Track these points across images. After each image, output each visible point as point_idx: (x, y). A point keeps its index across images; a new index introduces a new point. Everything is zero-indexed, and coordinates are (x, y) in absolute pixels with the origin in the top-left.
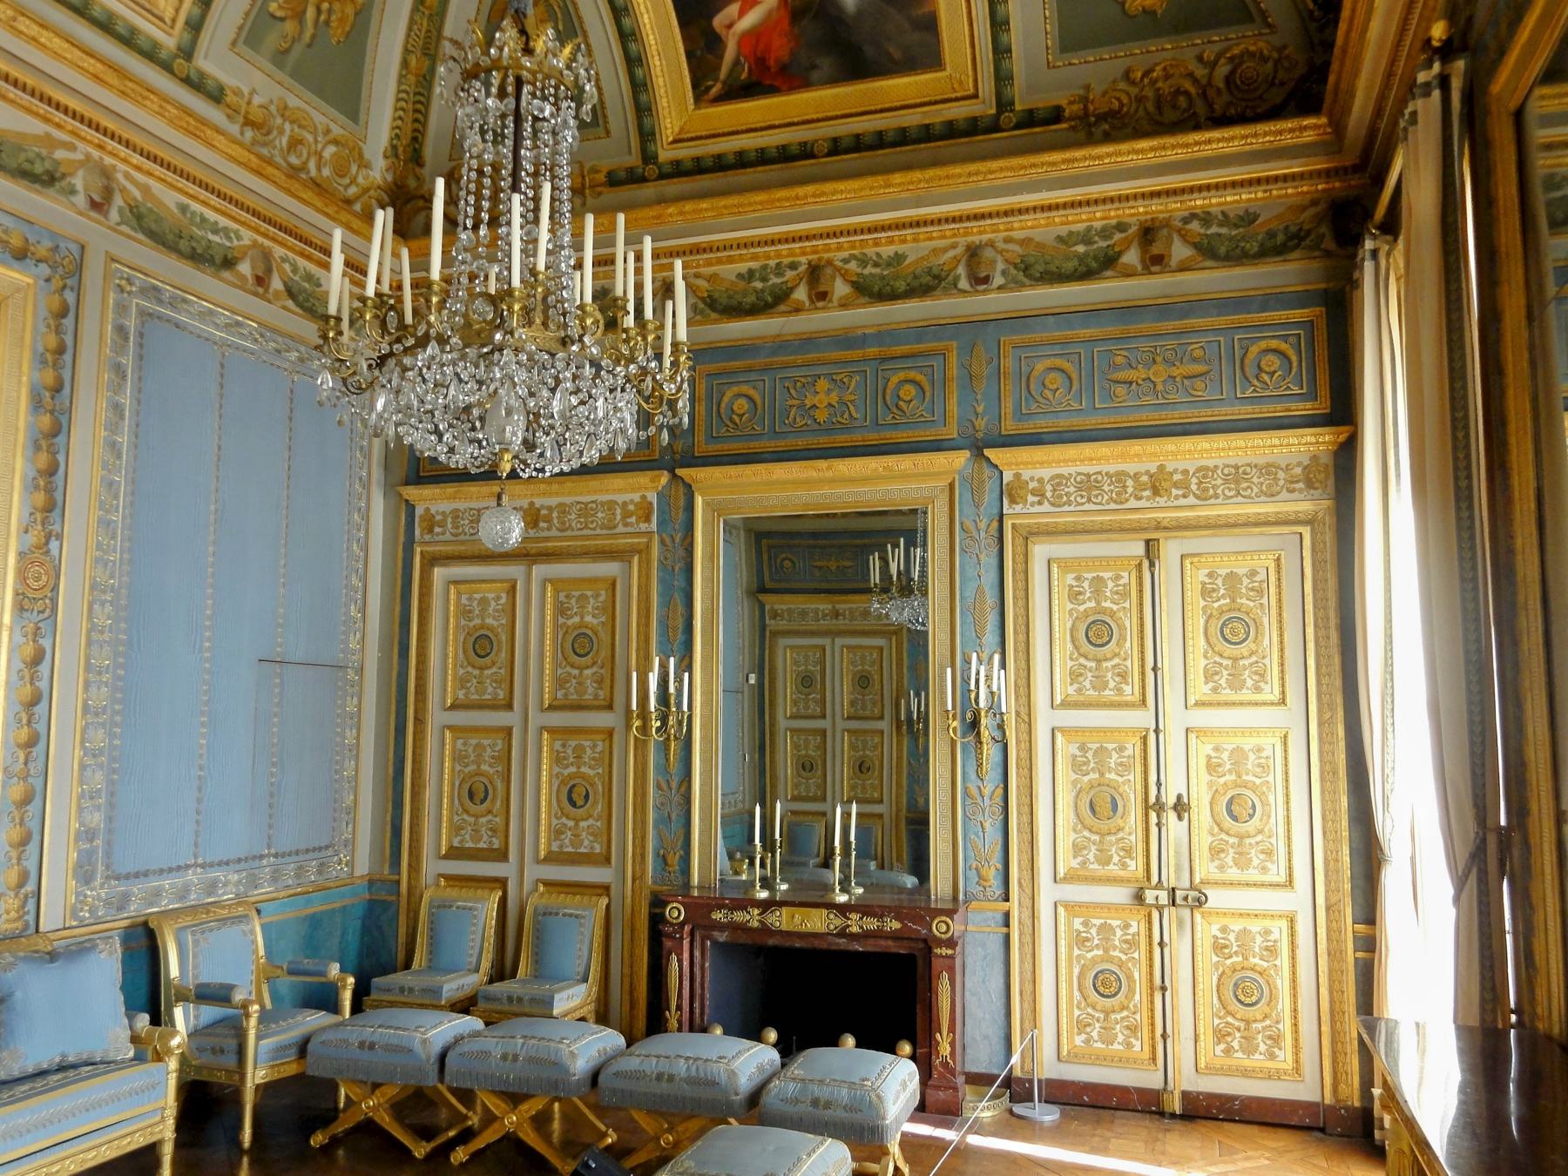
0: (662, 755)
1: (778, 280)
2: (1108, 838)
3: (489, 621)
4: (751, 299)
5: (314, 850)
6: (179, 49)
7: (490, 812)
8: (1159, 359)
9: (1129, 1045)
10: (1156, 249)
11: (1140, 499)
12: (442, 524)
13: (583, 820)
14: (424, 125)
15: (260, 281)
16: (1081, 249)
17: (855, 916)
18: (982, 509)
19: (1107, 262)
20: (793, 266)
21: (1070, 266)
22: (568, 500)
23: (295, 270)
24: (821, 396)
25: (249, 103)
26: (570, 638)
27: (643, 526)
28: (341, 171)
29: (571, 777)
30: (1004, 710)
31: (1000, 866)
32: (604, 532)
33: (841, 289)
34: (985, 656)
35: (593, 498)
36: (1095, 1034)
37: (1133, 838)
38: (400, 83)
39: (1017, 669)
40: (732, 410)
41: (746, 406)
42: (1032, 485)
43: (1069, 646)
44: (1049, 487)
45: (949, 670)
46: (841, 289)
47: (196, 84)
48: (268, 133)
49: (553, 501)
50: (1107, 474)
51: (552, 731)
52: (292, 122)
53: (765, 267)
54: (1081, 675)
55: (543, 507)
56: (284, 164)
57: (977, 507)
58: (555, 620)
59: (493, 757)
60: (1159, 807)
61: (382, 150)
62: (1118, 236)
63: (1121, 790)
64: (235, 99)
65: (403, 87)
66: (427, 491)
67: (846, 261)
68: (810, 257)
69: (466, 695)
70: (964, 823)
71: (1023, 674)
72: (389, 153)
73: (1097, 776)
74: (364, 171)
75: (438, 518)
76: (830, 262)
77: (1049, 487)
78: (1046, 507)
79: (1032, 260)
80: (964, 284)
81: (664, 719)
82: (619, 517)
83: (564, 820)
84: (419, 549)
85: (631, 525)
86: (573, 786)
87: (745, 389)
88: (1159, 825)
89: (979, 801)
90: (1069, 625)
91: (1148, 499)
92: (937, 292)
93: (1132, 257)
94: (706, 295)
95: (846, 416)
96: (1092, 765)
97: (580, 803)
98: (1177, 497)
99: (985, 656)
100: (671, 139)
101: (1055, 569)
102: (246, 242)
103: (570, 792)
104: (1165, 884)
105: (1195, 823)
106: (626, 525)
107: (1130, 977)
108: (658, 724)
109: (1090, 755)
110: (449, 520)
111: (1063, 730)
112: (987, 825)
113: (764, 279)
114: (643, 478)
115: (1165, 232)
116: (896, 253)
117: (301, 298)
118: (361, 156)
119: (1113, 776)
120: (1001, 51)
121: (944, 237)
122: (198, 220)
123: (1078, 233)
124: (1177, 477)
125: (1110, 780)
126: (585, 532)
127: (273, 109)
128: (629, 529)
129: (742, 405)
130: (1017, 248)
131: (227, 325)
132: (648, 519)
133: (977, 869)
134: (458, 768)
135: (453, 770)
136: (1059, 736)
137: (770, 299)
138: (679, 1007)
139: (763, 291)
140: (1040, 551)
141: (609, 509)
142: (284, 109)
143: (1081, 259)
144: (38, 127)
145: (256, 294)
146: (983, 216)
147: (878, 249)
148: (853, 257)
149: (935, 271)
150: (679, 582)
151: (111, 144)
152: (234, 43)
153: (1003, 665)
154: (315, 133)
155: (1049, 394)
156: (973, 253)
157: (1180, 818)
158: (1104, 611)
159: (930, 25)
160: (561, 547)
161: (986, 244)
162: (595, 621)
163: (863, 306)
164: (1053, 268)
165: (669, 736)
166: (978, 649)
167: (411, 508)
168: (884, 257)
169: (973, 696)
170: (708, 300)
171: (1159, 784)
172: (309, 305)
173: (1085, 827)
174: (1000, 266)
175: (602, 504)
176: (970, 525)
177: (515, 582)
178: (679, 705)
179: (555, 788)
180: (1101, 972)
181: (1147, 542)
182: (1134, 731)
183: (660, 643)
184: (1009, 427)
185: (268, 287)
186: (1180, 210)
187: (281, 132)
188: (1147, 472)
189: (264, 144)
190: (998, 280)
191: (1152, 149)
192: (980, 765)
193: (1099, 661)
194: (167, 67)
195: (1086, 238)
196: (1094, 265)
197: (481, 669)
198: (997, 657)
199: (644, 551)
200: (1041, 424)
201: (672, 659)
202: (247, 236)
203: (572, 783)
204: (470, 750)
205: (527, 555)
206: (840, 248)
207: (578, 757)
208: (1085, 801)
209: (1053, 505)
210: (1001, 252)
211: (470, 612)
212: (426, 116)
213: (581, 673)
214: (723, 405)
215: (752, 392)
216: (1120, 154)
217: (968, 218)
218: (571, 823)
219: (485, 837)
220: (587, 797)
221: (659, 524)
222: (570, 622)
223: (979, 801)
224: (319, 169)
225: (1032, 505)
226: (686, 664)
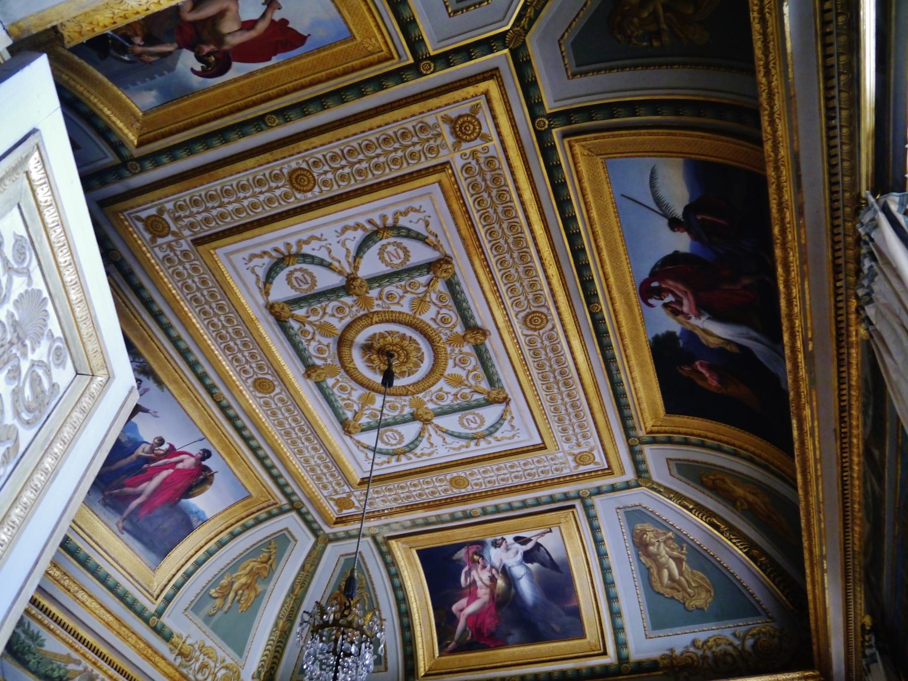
6: (156, 611)
25: (184, 643)
38: (271, 635)
47: (160, 631)
65: (272, 638)
72: (255, 676)
120: (618, 630)
127: (196, 646)
142: (201, 649)
144: (64, 650)
151: (101, 662)
152: (186, 610)
154: (216, 662)
159: (576, 612)
187: (197, 660)
189: (186, 667)
194: (146, 621)
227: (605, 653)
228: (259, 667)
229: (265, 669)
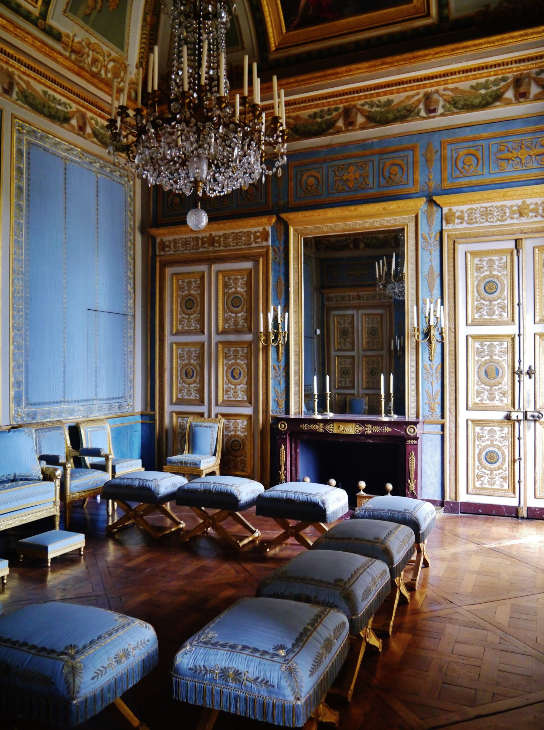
0: (275, 353)
1: (329, 117)
2: (494, 388)
3: (192, 292)
7: (195, 382)
8: (523, 147)
9: (502, 486)
10: (522, 90)
11: (512, 218)
12: (169, 247)
16: (483, 91)
17: (369, 426)
18: (432, 227)
19: (497, 97)
20: (336, 109)
21: (477, 101)
22: (228, 232)
24: (351, 175)
26: (230, 299)
27: (264, 243)
29: (232, 365)
30: (443, 326)
31: (440, 403)
32: (246, 247)
33: (360, 119)
34: (434, 301)
35: (240, 230)
36: (486, 481)
37: (506, 387)
38: (143, 29)
39: (449, 306)
40: (307, 184)
41: (314, 182)
42: (457, 214)
43: (476, 294)
44: (466, 215)
45: (415, 307)
46: (360, 119)
49: (221, 233)
50: (496, 207)
53: (322, 111)
54: (481, 308)
55: (216, 236)
57: (430, 226)
58: (223, 290)
59: (196, 356)
60: (520, 373)
62: (502, 84)
63: (501, 364)
66: (161, 231)
67: (363, 105)
69: (182, 327)
70: (423, 383)
71: (453, 309)
72: (138, 65)
73: (489, 358)
75: (167, 243)
76: (355, 106)
77: (466, 215)
78: (465, 225)
79: (458, 99)
80: (423, 113)
81: (276, 335)
82: (252, 239)
83: (230, 385)
84: (158, 259)
85: (258, 243)
86: (234, 369)
87: (313, 173)
88: (519, 381)
89: (430, 371)
90: (476, 284)
91: (517, 218)
92: (409, 119)
93: (510, 94)
95: (364, 183)
96: (486, 353)
97: (237, 377)
98: (532, 217)
99: (434, 301)
101: (469, 256)
103: (232, 372)
104: (522, 410)
105: (537, 380)
106: (256, 243)
107: (503, 454)
108: (273, 338)
109: (485, 348)
110: (172, 244)
111: (472, 337)
112: (434, 384)
113: (322, 117)
114: (264, 220)
115: (527, 80)
116: (388, 100)
119: (496, 357)
121: (412, 90)
123: (482, 83)
124: (532, 207)
125: (495, 359)
128: (258, 245)
129: (312, 180)
130: (450, 93)
132: (267, 240)
133: (428, 404)
136: (470, 339)
137: (324, 127)
139: (321, 123)
140: (461, 249)
141: (248, 235)
143: (483, 96)
146: (432, 78)
147: (379, 98)
148: (366, 103)
149: (408, 108)
150: (282, 270)
153: (442, 304)
155: (467, 167)
157: (530, 377)
158: (493, 276)
160: (225, 255)
161: (434, 92)
162: (242, 290)
163: (372, 127)
164: (469, 102)
165: (278, 344)
166: (430, 297)
167: (154, 239)
168: (382, 101)
169: (427, 320)
170: (294, 129)
171: (520, 361)
173: (482, 383)
174: (441, 103)
175: (244, 233)
177: (204, 273)
178: (283, 328)
180: (489, 452)
181: (516, 240)
182: (508, 336)
183: (274, 300)
184: (446, 185)
186: (534, 68)
188: (517, 205)
190: (440, 110)
191: (521, 36)
192: (430, 354)
193: (491, 301)
195: (486, 86)
196: (490, 99)
197: (189, 315)
198: (439, 300)
200: (463, 181)
201: (279, 307)
203: (233, 368)
204: (185, 353)
206: (359, 98)
207: (235, 356)
208: (483, 370)
209: (468, 223)
210: (442, 96)
211: (183, 288)
215: (316, 174)
216: (504, 39)
217: (425, 79)
218: (233, 387)
219: (193, 394)
220: (240, 374)
221: (273, 241)
222: (230, 291)
223: (430, 371)
225: (458, 224)
226: (286, 308)
227: (428, 15)
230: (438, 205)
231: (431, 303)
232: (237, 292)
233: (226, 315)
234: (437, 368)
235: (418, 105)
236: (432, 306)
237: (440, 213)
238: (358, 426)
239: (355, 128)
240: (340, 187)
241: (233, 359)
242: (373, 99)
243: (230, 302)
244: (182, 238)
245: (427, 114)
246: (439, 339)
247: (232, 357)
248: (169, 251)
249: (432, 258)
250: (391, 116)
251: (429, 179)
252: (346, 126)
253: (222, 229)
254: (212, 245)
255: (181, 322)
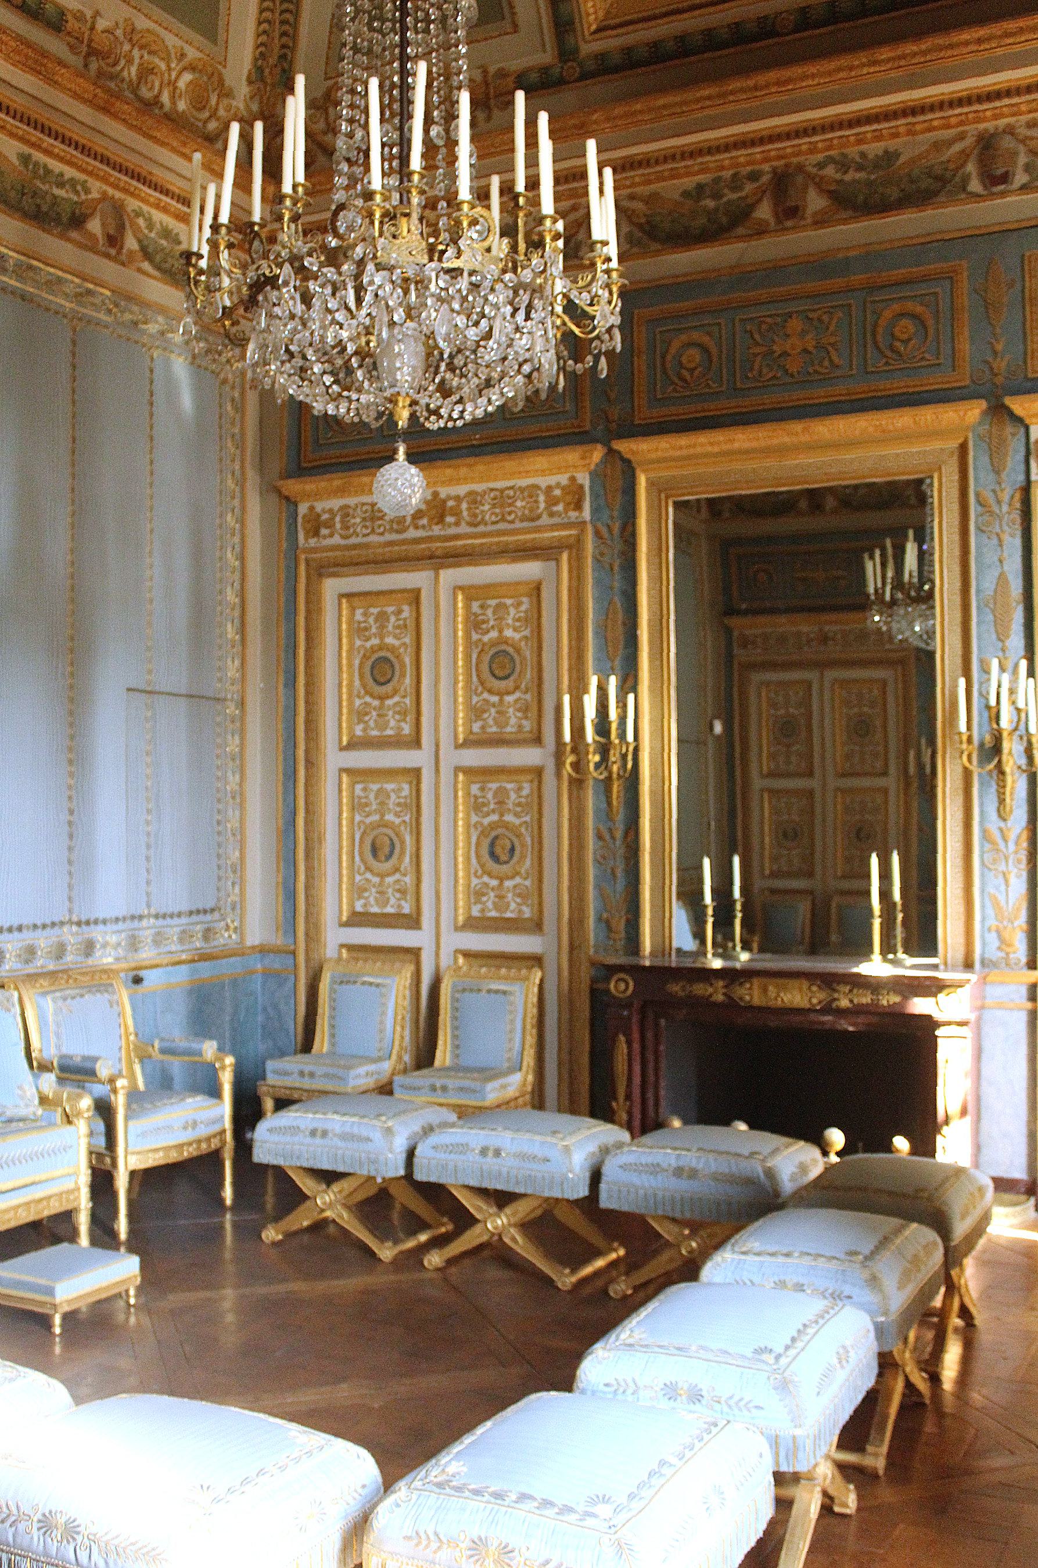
0: (603, 798)
1: (734, 196)
3: (390, 640)
4: (702, 221)
5: (198, 912)
7: (397, 870)
12: (329, 524)
13: (508, 878)
14: (295, 38)
15: (114, 240)
18: (1004, 475)
20: (754, 176)
23: (150, 226)
25: (92, 28)
26: (486, 658)
27: (573, 514)
28: (199, 103)
29: (493, 826)
33: (815, 202)
34: (1010, 666)
40: (680, 363)
45: (962, 682)
46: (815, 202)
48: (115, 65)
49: (462, 490)
51: (469, 771)
52: (141, 48)
53: (717, 180)
55: (449, 498)
56: (131, 96)
57: (997, 472)
59: (399, 804)
61: (245, 72)
64: (77, 25)
66: (309, 485)
67: (821, 166)
68: (775, 163)
69: (365, 730)
74: (226, 101)
75: (325, 517)
76: (800, 168)
80: (975, 185)
81: (604, 750)
86: (496, 838)
87: (695, 335)
94: (643, 220)
95: (826, 363)
97: (504, 858)
99: (1010, 666)
100: (594, 27)
102: (95, 195)
103: (492, 844)
108: (597, 758)
110: (338, 519)
113: (717, 196)
114: (571, 456)
116: (886, 152)
117: (158, 258)
118: (221, 81)
121: (948, 127)
122: (41, 171)
126: (502, 526)
127: (119, 33)
131: (78, 295)
132: (578, 506)
133: (998, 931)
134: (358, 818)
135: (352, 821)
138: (628, 1097)
139: (716, 210)
141: (531, 496)
145: (107, 256)
147: (864, 147)
148: (831, 160)
149: (938, 171)
154: (167, 60)
156: (987, 144)
161: (1004, 131)
162: (517, 636)
163: (845, 221)
166: (1000, 654)
170: (647, 228)
172: (167, 266)
174: (1022, 159)
175: (522, 490)
176: (991, 500)
179: (474, 840)
183: (598, 660)
185: (121, 248)
187: (130, 61)
192: (1002, 801)
197: (382, 698)
198: (1023, 664)
199: (575, 547)
202: (97, 188)
203: (493, 834)
204: (372, 796)
205: (431, 558)
206: (813, 150)
207: (500, 803)
211: (366, 629)
212: (295, 26)
213: (501, 700)
214: (669, 357)
215: (706, 340)
218: (494, 883)
219: (392, 901)
220: (512, 850)
221: (595, 511)
224: (174, 103)
226: (629, 682)
228: (256, 60)
229: (271, 61)
230: (1019, 420)
231: (1002, 669)
232: (502, 640)
233: (475, 699)
234: (1019, 837)
235: (963, 165)
236: (1006, 678)
237: (1023, 440)
238: (814, 988)
239: (802, 223)
240: (765, 371)
241: (493, 811)
242: (845, 151)
243: (485, 667)
244: (363, 504)
245: (985, 187)
246: (1023, 762)
247: (492, 806)
248: (331, 535)
249: (1005, 554)
250: (894, 193)
251: (995, 353)
252: (779, 221)
253: (465, 480)
254: (440, 519)
255: (360, 715)
